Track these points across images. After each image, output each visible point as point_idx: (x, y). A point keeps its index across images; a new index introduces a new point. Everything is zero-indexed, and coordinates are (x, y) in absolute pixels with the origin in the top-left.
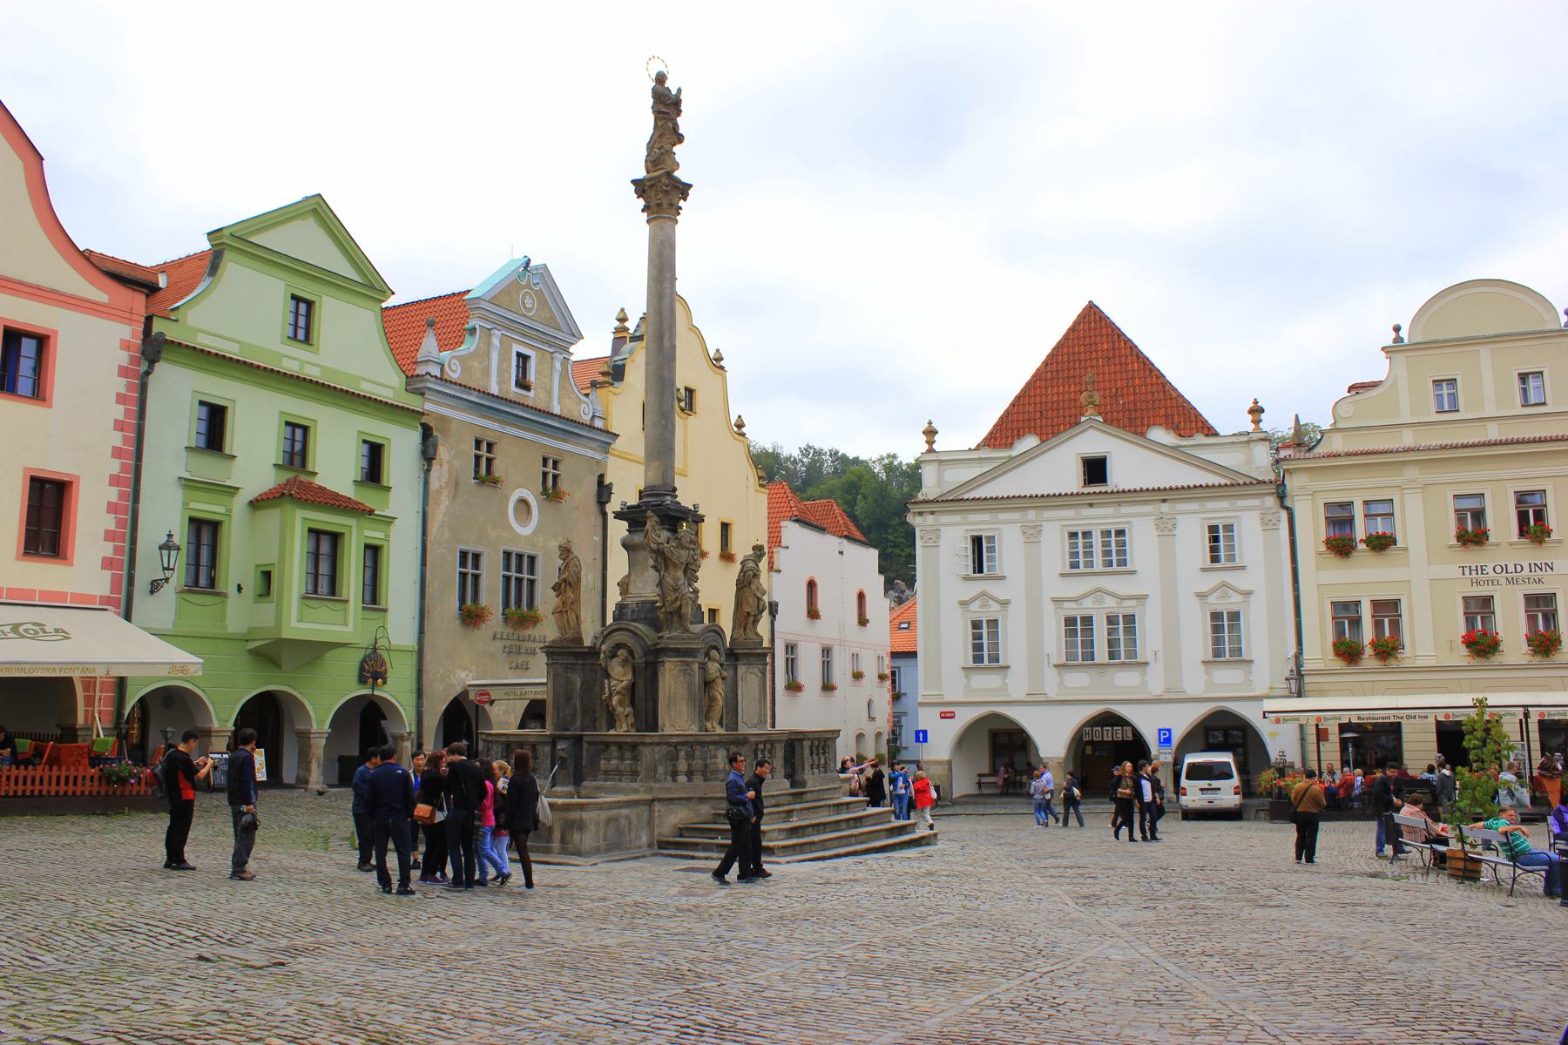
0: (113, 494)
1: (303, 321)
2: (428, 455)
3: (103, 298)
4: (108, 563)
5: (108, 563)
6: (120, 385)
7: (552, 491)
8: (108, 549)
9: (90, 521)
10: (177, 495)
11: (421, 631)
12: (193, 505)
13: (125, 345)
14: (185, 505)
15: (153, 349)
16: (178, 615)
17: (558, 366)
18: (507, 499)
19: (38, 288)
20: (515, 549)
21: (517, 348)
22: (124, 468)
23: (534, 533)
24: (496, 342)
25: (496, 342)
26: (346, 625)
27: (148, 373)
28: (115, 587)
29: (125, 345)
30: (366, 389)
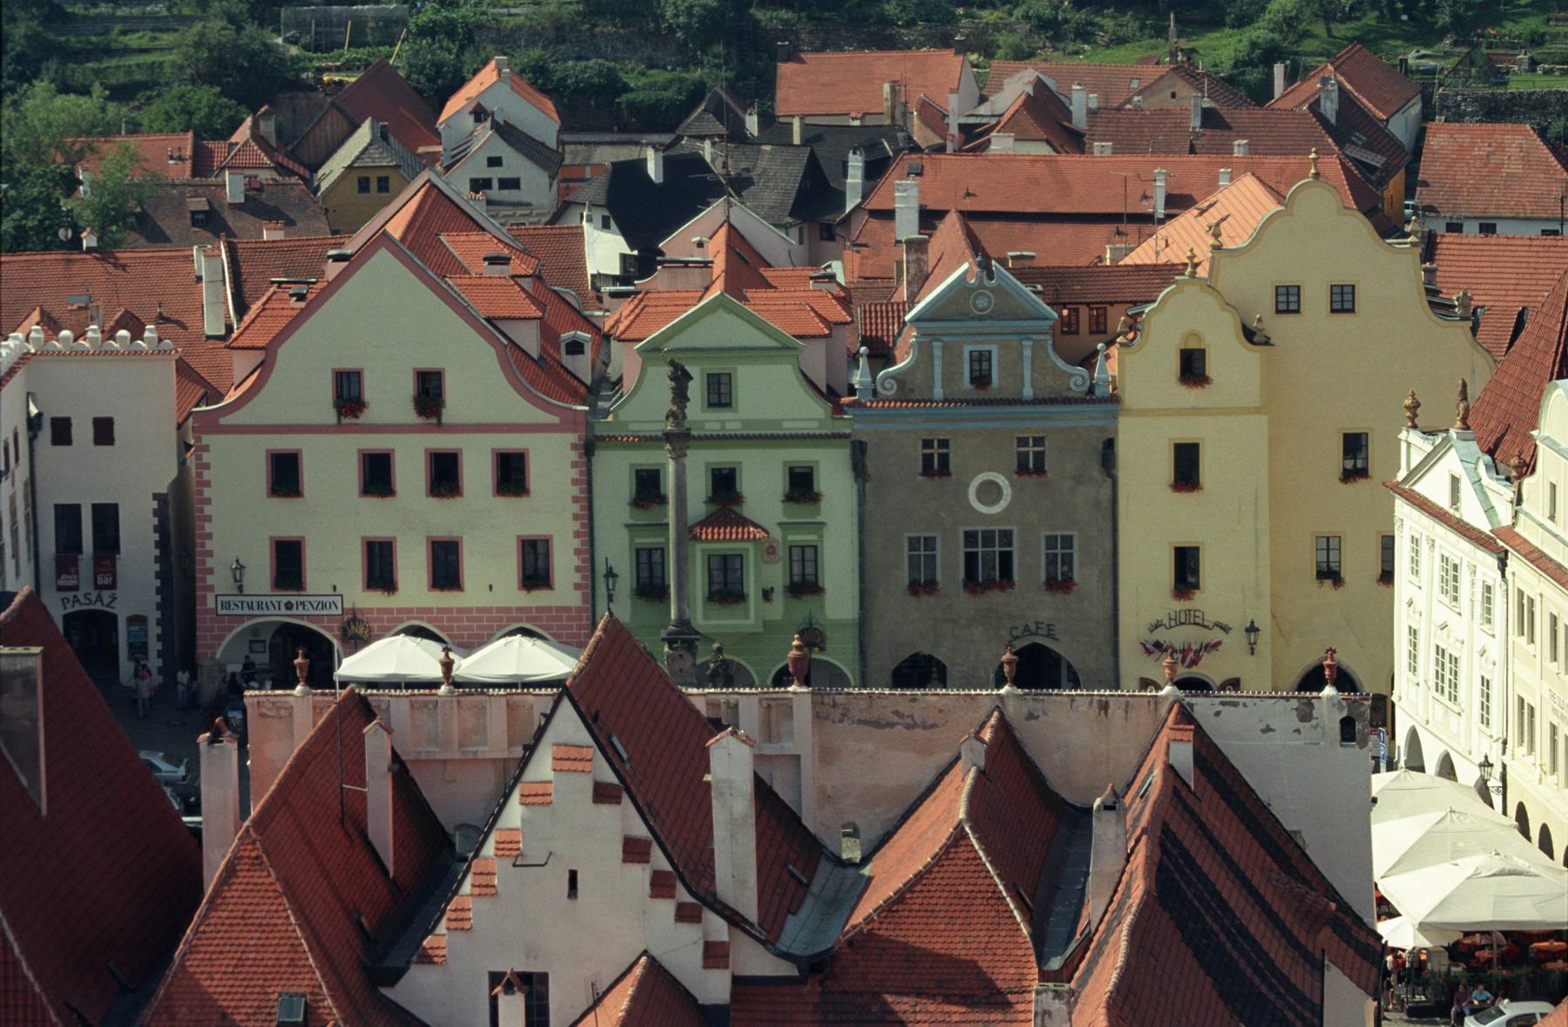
0: (576, 543)
1: (720, 393)
2: (859, 470)
3: (555, 419)
4: (577, 586)
5: (577, 586)
6: (574, 473)
7: (1030, 467)
8: (577, 578)
9: (564, 563)
10: (624, 534)
11: (862, 606)
12: (637, 540)
13: (574, 447)
14: (631, 540)
15: (589, 448)
16: (634, 613)
17: (1027, 353)
18: (968, 486)
19: (508, 425)
20: (980, 528)
21: (967, 349)
22: (583, 526)
23: (1006, 510)
24: (938, 353)
25: (938, 353)
26: (747, 617)
27: (589, 461)
28: (584, 600)
29: (574, 447)
30: (789, 427)
